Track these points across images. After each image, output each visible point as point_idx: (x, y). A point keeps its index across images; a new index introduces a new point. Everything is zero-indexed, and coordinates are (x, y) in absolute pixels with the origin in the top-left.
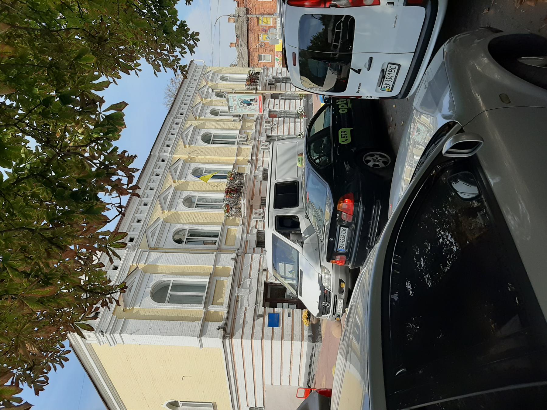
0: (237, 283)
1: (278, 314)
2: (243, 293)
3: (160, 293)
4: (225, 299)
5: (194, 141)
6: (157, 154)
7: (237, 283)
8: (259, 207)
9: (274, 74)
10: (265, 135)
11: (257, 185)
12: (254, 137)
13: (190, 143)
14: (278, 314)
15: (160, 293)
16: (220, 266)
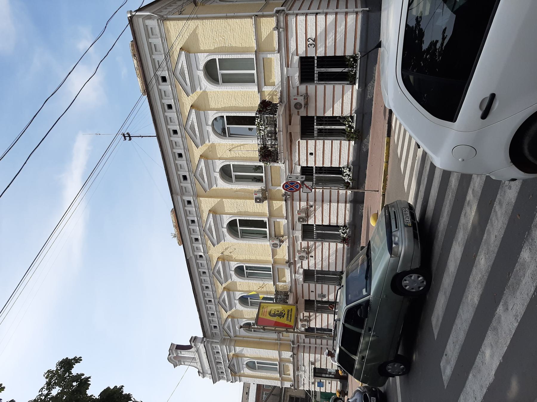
0: (297, 368)
1: (323, 382)
2: (301, 373)
3: (251, 366)
4: (291, 372)
5: (222, 237)
6: (192, 255)
7: (297, 368)
8: (304, 310)
9: (302, 52)
10: (299, 226)
11: (299, 288)
12: (287, 232)
13: (219, 242)
14: (323, 382)
15: (251, 366)
16: (277, 257)
